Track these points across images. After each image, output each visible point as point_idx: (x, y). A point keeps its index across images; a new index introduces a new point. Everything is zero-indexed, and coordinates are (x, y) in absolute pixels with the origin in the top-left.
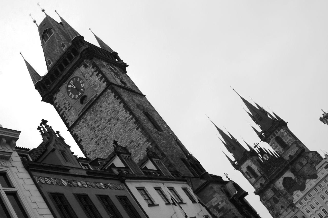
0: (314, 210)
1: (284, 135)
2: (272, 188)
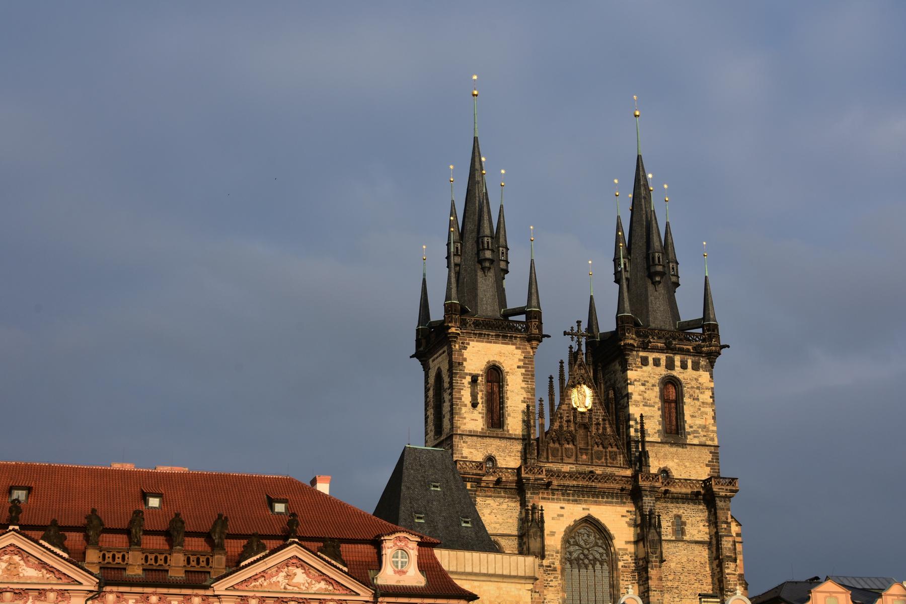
1: (701, 397)
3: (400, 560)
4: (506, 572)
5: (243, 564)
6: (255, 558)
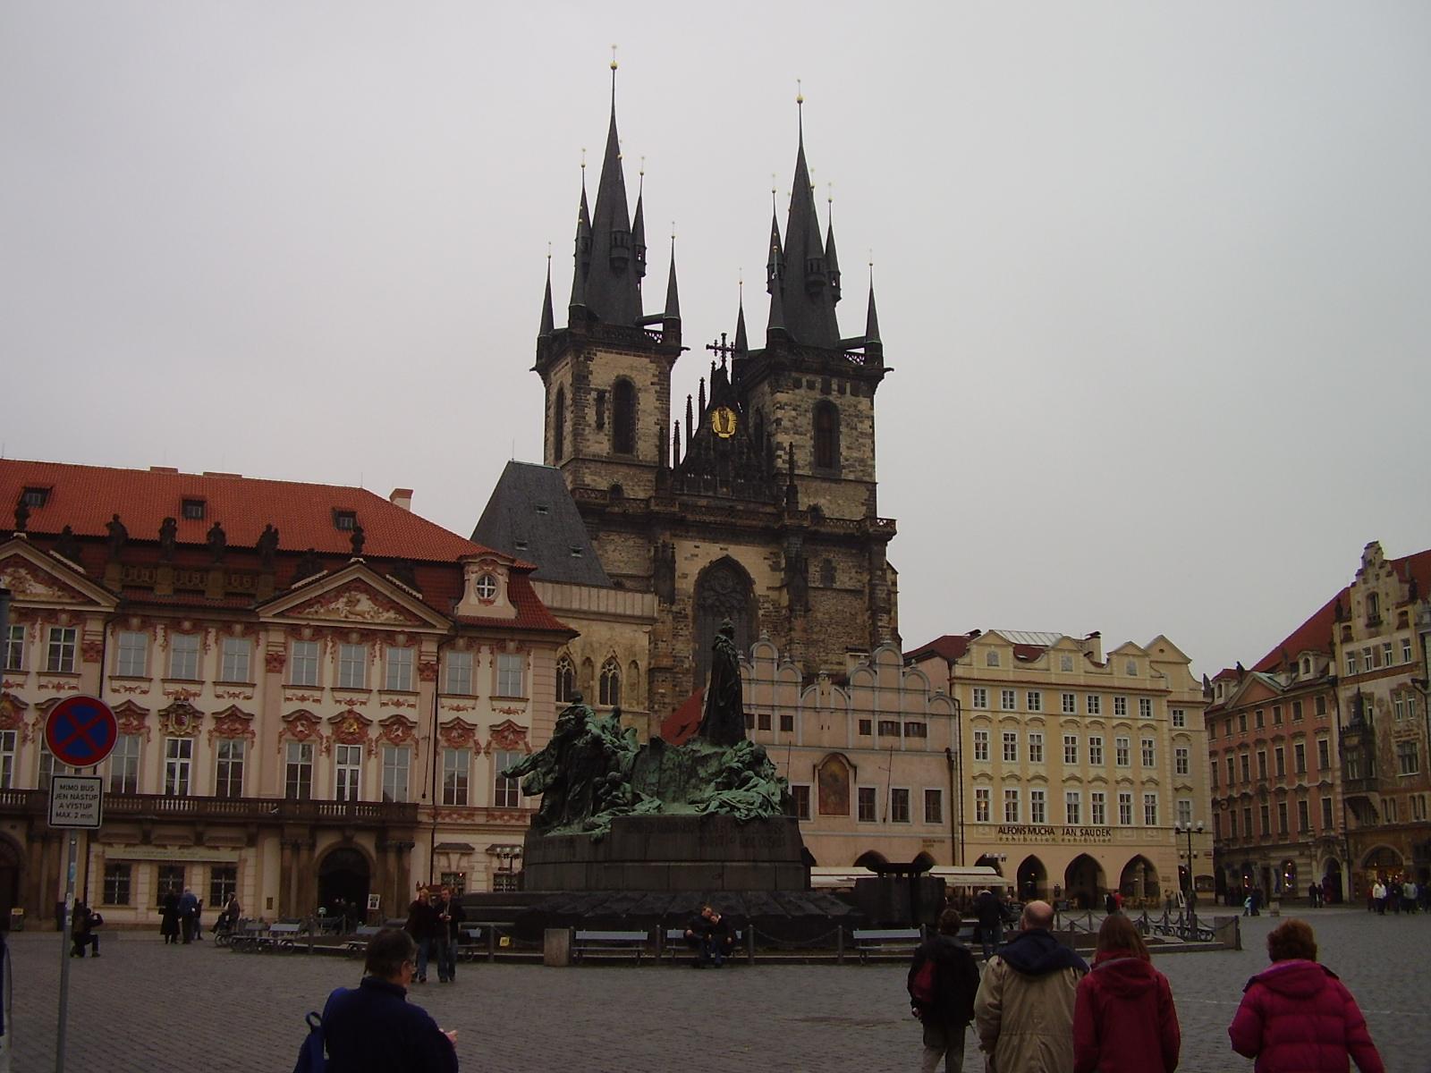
0: (1008, 767)
1: (859, 425)
2: (665, 545)
3: (486, 587)
4: (620, 610)
5: (293, 587)
6: (310, 579)
